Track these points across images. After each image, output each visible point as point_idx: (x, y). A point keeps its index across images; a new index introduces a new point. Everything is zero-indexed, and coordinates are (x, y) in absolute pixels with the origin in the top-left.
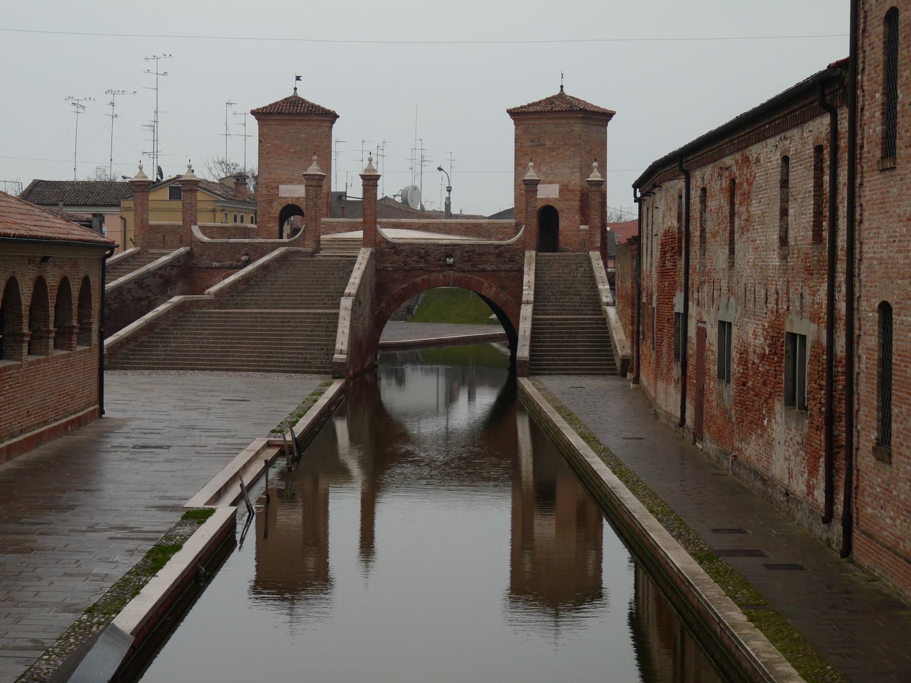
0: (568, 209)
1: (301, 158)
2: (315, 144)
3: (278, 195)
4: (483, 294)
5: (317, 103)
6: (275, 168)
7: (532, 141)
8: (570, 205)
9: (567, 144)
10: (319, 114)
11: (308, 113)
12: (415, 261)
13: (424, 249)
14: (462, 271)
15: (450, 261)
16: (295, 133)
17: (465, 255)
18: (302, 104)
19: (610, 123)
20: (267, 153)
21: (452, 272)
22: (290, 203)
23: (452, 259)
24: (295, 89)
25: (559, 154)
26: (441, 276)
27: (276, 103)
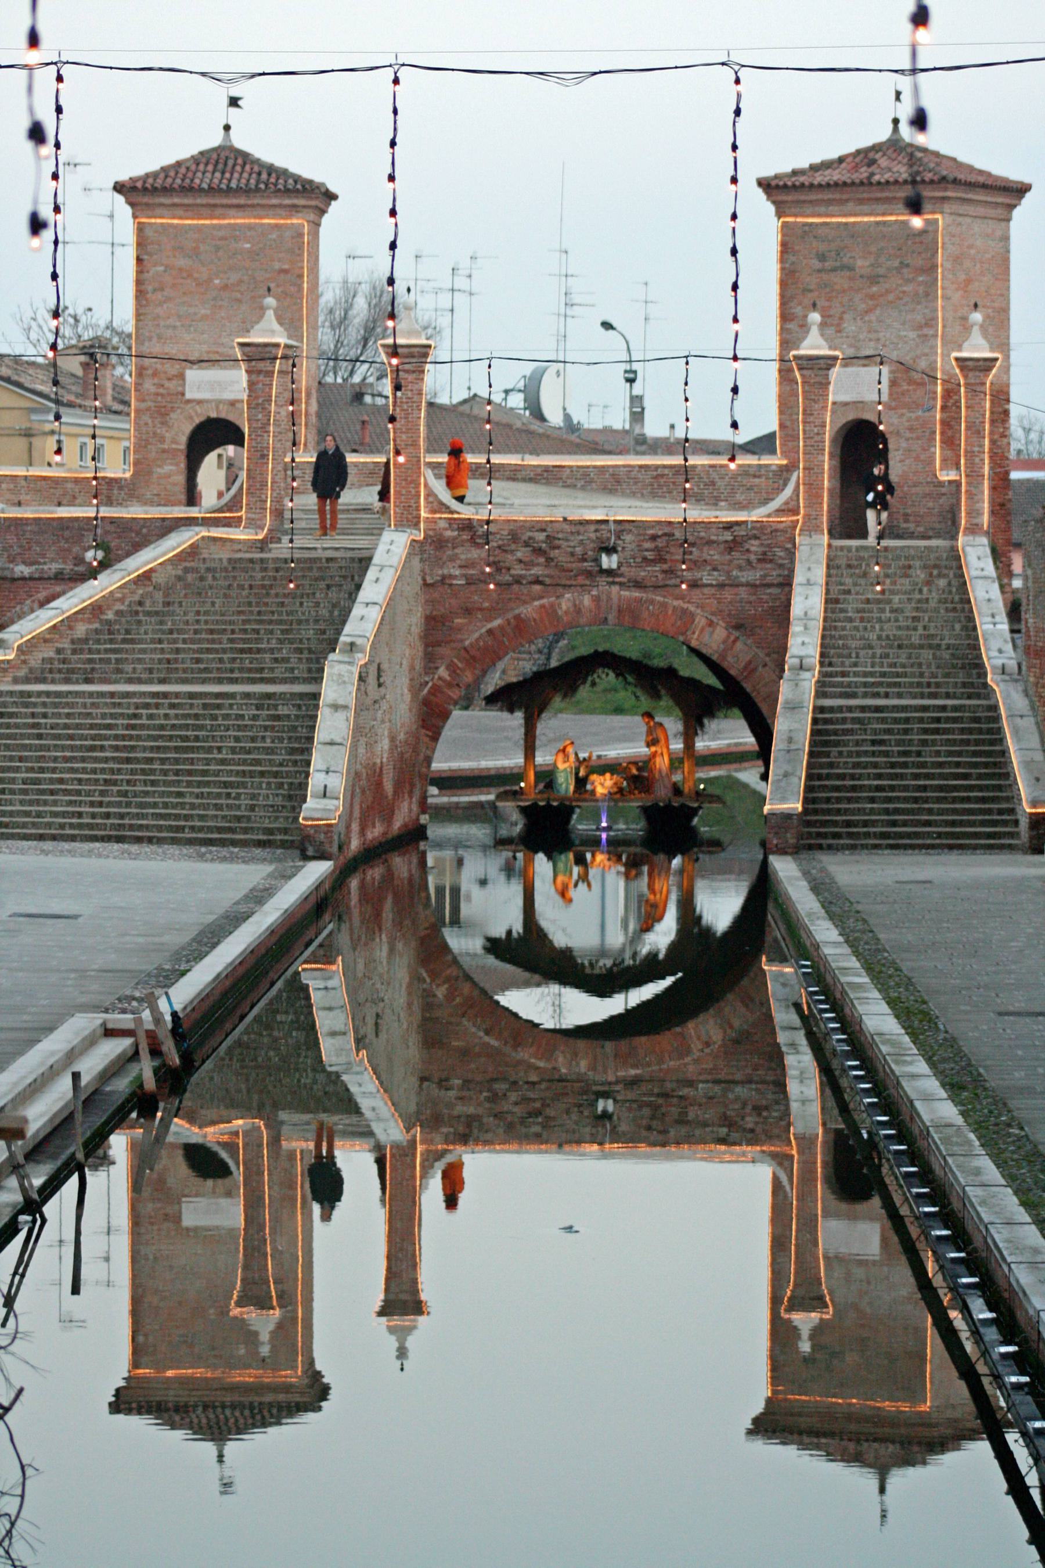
0: (911, 429)
1: (239, 301)
2: (277, 266)
3: (183, 394)
4: (694, 644)
5: (280, 162)
6: (175, 327)
7: (822, 258)
8: (917, 418)
9: (908, 266)
10: (287, 191)
11: (257, 189)
12: (520, 561)
13: (544, 530)
14: (638, 585)
15: (608, 562)
16: (222, 239)
17: (648, 545)
18: (245, 164)
19: (1017, 213)
20: (155, 290)
21: (615, 589)
22: (214, 415)
23: (615, 558)
24: (227, 128)
25: (888, 291)
26: (587, 601)
27: (178, 164)
